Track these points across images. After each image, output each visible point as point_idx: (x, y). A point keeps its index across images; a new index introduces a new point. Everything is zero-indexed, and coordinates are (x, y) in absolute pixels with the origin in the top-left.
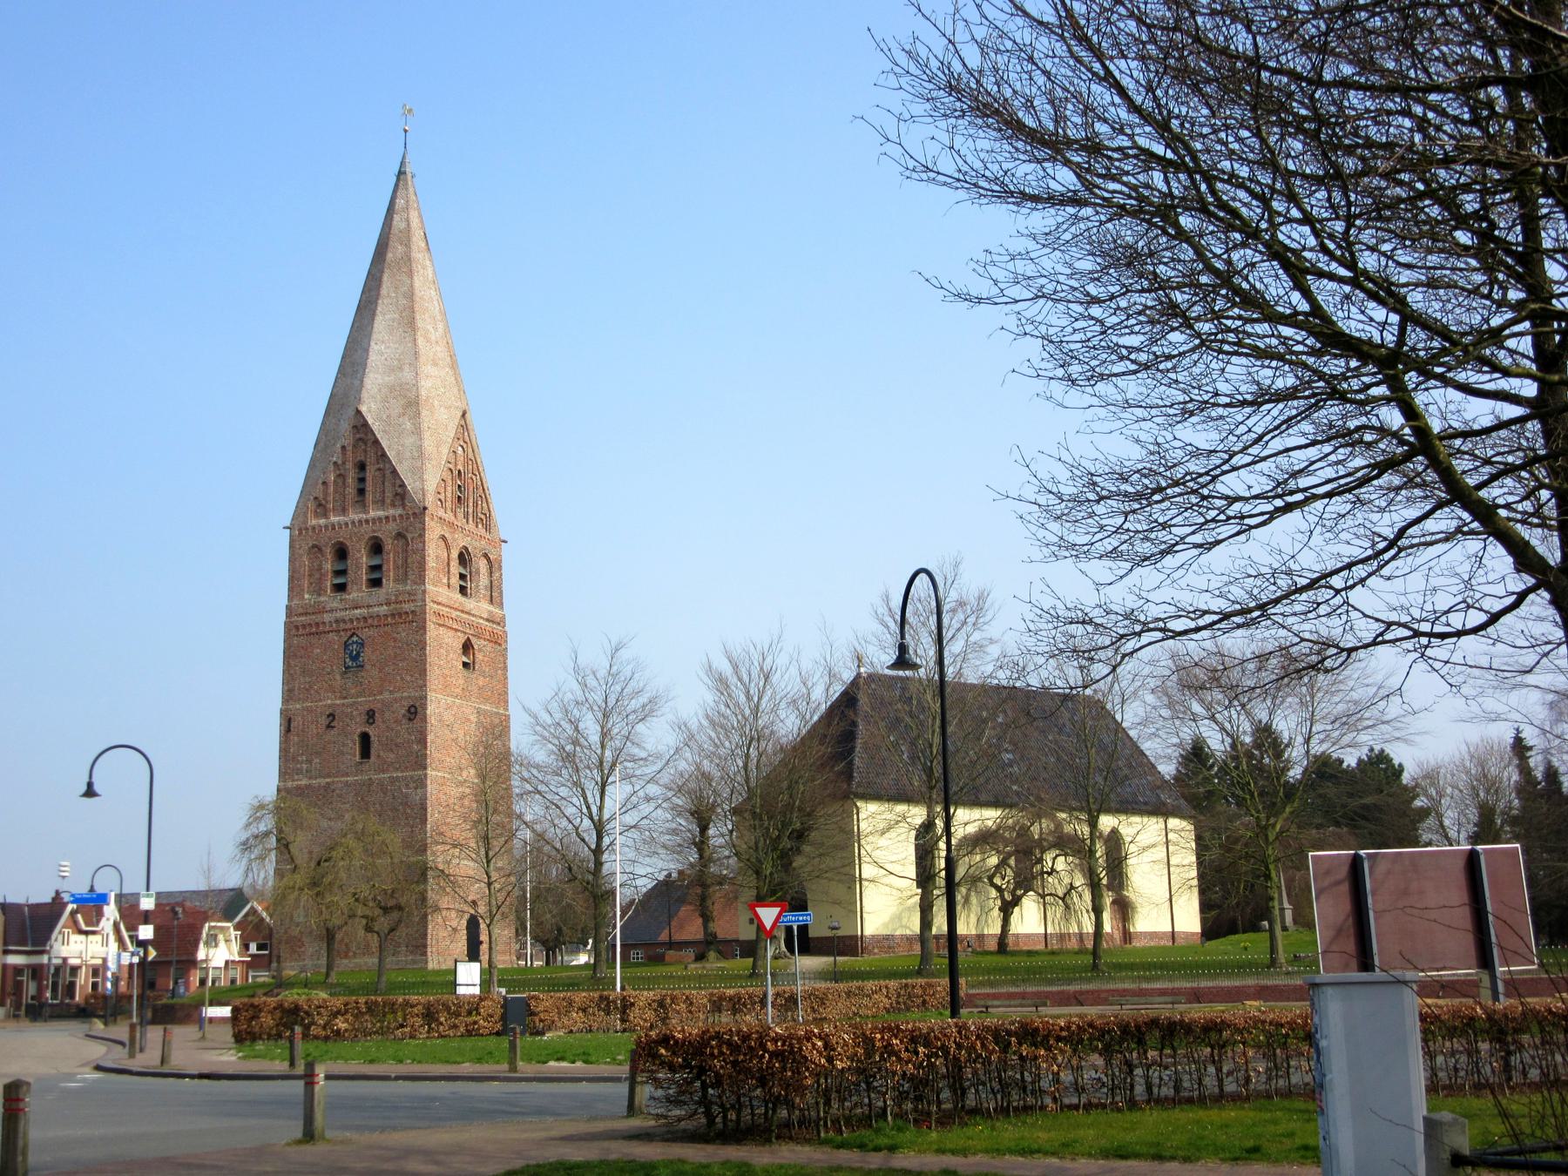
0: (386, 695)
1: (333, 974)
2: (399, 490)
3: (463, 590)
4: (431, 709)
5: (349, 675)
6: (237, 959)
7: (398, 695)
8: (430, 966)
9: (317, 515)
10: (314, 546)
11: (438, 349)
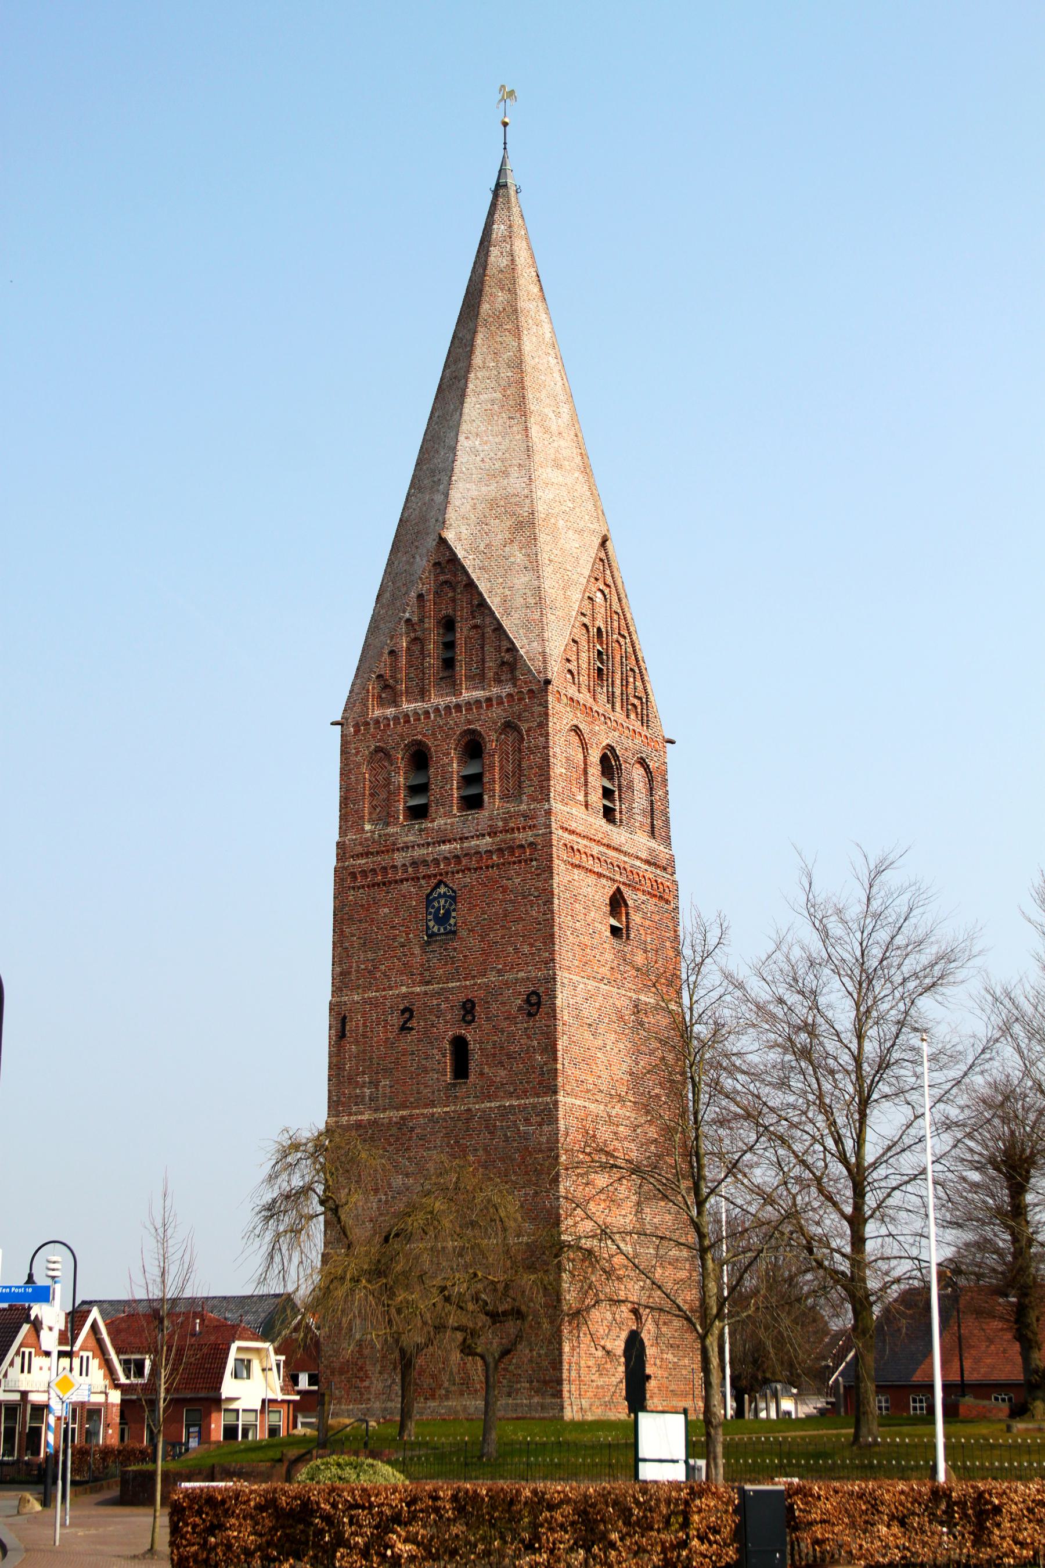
0: (492, 977)
1: (411, 1426)
2: (507, 657)
3: (609, 814)
4: (562, 998)
5: (434, 947)
6: (280, 1397)
7: (509, 976)
8: (568, 1414)
9: (382, 703)
10: (378, 750)
11: (562, 443)
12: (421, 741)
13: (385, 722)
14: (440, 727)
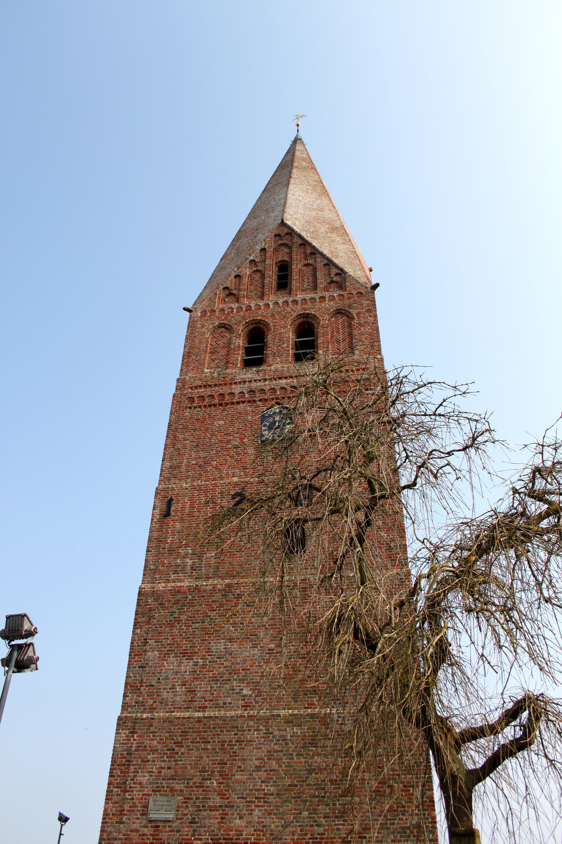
12: (261, 320)
13: (229, 310)
14: (278, 312)
